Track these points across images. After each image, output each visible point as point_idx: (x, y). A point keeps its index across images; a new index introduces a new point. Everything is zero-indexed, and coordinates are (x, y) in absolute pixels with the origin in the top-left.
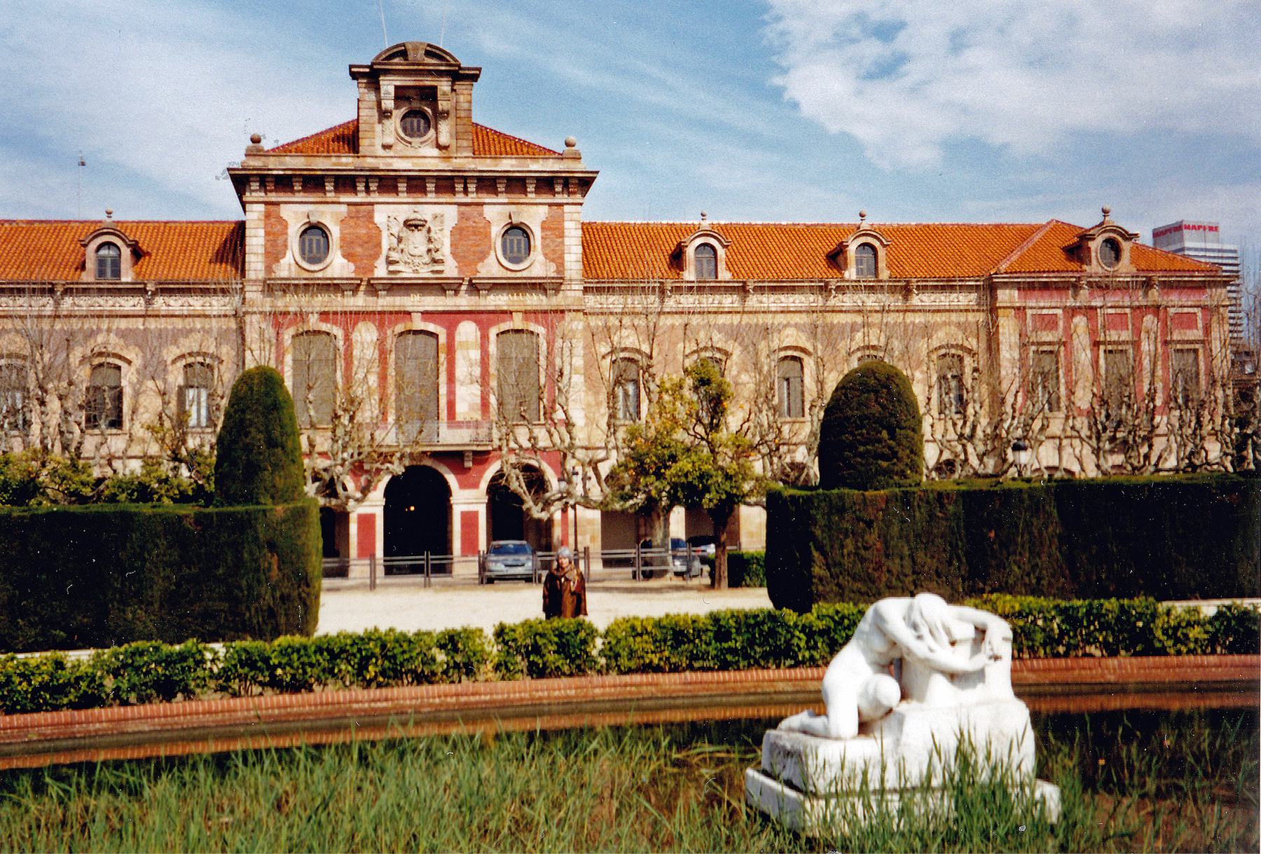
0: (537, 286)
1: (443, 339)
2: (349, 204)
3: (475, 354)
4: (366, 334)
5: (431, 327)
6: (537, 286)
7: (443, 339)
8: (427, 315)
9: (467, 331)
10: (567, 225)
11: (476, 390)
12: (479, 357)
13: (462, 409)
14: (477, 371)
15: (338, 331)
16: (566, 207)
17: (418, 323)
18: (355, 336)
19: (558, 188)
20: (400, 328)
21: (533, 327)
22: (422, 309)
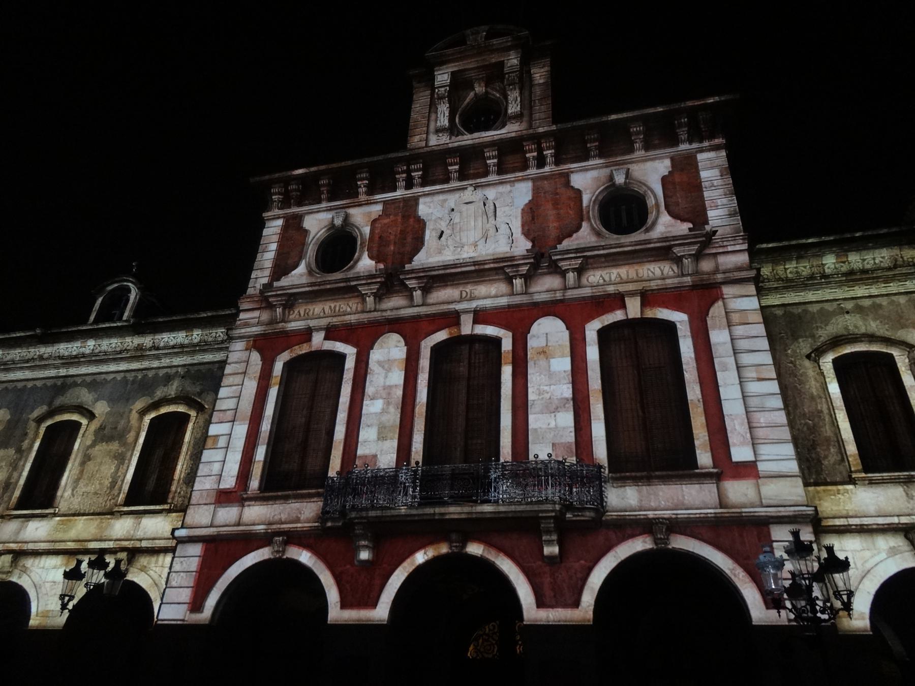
0: (663, 251)
1: (507, 345)
2: (385, 203)
3: (563, 364)
4: (390, 351)
5: (490, 330)
6: (663, 251)
7: (507, 345)
8: (480, 316)
9: (549, 331)
10: (704, 174)
11: (567, 419)
12: (568, 367)
13: (540, 451)
14: (566, 391)
15: (350, 351)
16: (700, 157)
17: (467, 328)
18: (376, 355)
19: (683, 134)
20: (441, 336)
21: (664, 314)
22: (474, 305)
